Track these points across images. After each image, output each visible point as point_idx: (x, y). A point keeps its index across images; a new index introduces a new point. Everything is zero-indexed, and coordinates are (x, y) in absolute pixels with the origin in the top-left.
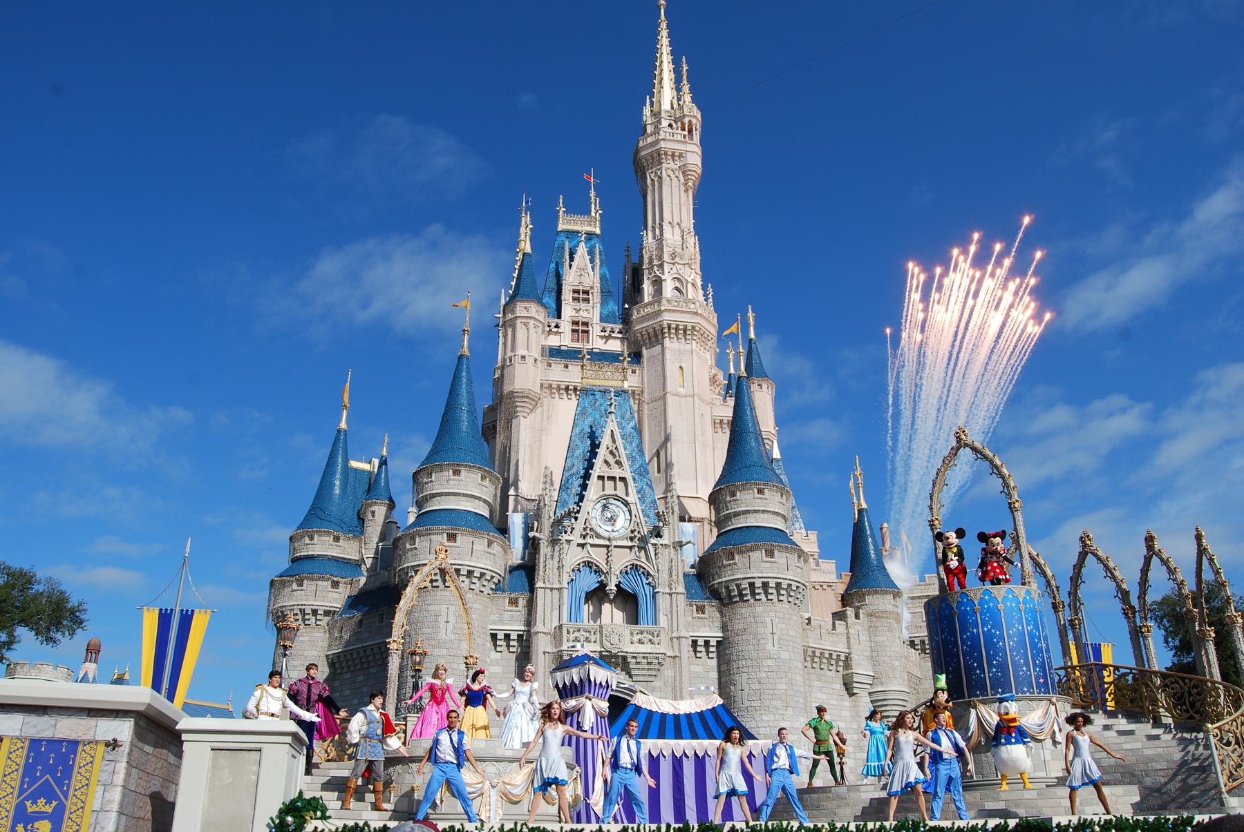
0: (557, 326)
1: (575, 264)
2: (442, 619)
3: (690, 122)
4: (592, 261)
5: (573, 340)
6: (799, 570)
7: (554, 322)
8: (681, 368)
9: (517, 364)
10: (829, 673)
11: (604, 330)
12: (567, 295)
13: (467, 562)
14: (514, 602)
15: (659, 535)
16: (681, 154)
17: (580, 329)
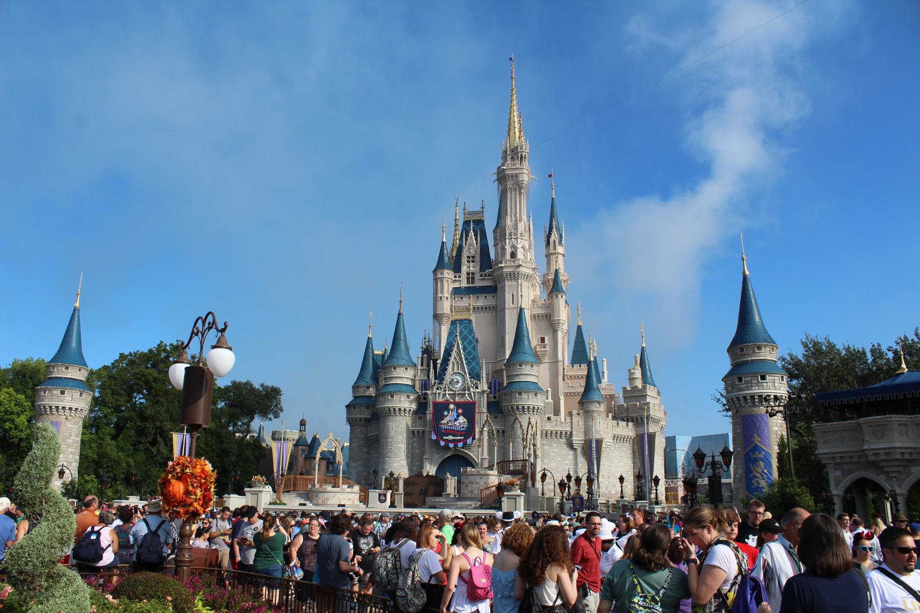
0: (460, 277)
1: (468, 242)
2: (390, 428)
3: (521, 155)
4: (476, 239)
5: (468, 283)
6: (534, 399)
7: (457, 275)
8: (513, 295)
9: (438, 302)
10: (561, 440)
11: (481, 276)
12: (464, 260)
13: (397, 405)
14: (420, 418)
15: (477, 388)
16: (516, 175)
17: (471, 277)
